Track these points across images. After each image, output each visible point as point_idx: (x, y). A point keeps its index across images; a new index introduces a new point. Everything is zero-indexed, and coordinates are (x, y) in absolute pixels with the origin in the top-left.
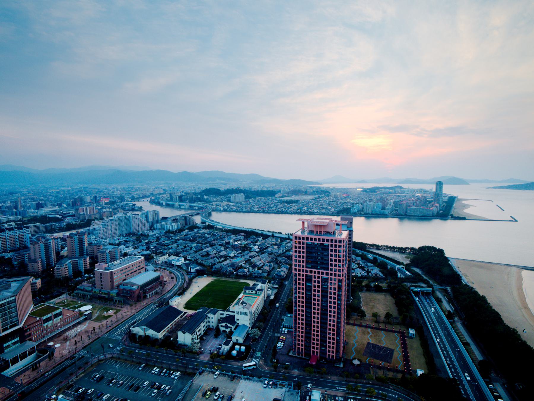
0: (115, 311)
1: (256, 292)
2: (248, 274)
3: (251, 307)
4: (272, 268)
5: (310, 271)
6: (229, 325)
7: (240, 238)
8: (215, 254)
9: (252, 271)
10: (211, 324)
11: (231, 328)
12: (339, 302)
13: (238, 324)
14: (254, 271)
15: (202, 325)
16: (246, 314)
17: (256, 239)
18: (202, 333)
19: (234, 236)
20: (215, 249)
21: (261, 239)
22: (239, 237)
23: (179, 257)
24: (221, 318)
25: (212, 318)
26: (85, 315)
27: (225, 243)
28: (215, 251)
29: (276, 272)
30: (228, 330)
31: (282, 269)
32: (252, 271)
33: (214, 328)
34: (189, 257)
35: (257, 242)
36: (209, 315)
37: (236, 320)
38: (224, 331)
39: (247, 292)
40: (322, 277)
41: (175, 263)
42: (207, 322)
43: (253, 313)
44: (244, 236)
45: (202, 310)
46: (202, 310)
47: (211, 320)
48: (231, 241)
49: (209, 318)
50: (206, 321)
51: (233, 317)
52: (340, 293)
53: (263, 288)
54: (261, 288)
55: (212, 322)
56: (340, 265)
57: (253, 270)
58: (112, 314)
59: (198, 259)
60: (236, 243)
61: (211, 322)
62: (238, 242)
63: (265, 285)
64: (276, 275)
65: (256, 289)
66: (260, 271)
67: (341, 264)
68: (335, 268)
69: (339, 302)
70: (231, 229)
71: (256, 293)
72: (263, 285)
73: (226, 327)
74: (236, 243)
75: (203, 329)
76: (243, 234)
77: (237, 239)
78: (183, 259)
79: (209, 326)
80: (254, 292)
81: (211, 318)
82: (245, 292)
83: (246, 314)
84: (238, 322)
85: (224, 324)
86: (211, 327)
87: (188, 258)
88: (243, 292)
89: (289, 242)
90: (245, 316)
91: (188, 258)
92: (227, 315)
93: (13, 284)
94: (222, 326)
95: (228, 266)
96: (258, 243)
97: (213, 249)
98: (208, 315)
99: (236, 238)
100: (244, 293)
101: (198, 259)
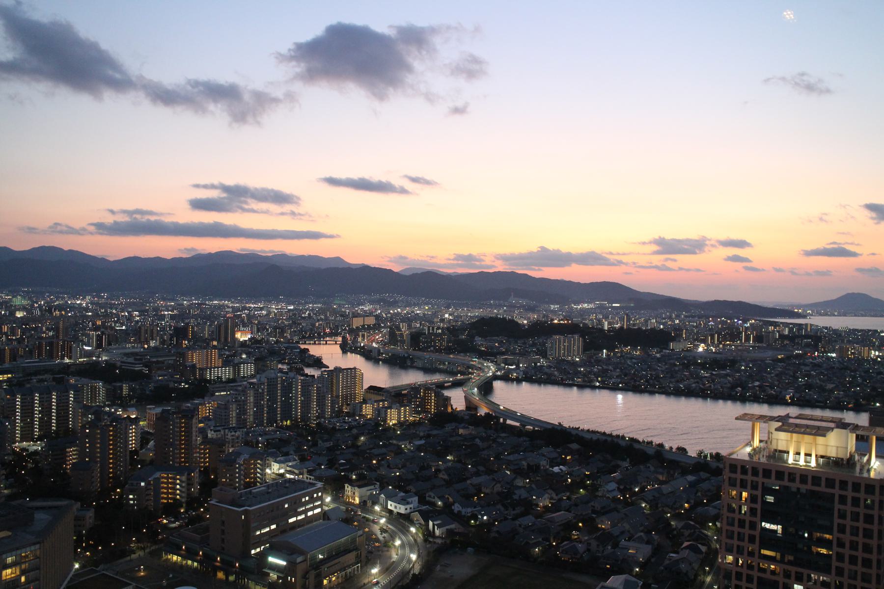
20: (500, 482)
23: (406, 492)
27: (526, 467)
34: (430, 496)
41: (396, 507)
48: (543, 463)
60: (556, 469)
62: (561, 467)
74: (556, 469)
78: (416, 499)
87: (427, 498)
89: (708, 479)
97: (494, 479)
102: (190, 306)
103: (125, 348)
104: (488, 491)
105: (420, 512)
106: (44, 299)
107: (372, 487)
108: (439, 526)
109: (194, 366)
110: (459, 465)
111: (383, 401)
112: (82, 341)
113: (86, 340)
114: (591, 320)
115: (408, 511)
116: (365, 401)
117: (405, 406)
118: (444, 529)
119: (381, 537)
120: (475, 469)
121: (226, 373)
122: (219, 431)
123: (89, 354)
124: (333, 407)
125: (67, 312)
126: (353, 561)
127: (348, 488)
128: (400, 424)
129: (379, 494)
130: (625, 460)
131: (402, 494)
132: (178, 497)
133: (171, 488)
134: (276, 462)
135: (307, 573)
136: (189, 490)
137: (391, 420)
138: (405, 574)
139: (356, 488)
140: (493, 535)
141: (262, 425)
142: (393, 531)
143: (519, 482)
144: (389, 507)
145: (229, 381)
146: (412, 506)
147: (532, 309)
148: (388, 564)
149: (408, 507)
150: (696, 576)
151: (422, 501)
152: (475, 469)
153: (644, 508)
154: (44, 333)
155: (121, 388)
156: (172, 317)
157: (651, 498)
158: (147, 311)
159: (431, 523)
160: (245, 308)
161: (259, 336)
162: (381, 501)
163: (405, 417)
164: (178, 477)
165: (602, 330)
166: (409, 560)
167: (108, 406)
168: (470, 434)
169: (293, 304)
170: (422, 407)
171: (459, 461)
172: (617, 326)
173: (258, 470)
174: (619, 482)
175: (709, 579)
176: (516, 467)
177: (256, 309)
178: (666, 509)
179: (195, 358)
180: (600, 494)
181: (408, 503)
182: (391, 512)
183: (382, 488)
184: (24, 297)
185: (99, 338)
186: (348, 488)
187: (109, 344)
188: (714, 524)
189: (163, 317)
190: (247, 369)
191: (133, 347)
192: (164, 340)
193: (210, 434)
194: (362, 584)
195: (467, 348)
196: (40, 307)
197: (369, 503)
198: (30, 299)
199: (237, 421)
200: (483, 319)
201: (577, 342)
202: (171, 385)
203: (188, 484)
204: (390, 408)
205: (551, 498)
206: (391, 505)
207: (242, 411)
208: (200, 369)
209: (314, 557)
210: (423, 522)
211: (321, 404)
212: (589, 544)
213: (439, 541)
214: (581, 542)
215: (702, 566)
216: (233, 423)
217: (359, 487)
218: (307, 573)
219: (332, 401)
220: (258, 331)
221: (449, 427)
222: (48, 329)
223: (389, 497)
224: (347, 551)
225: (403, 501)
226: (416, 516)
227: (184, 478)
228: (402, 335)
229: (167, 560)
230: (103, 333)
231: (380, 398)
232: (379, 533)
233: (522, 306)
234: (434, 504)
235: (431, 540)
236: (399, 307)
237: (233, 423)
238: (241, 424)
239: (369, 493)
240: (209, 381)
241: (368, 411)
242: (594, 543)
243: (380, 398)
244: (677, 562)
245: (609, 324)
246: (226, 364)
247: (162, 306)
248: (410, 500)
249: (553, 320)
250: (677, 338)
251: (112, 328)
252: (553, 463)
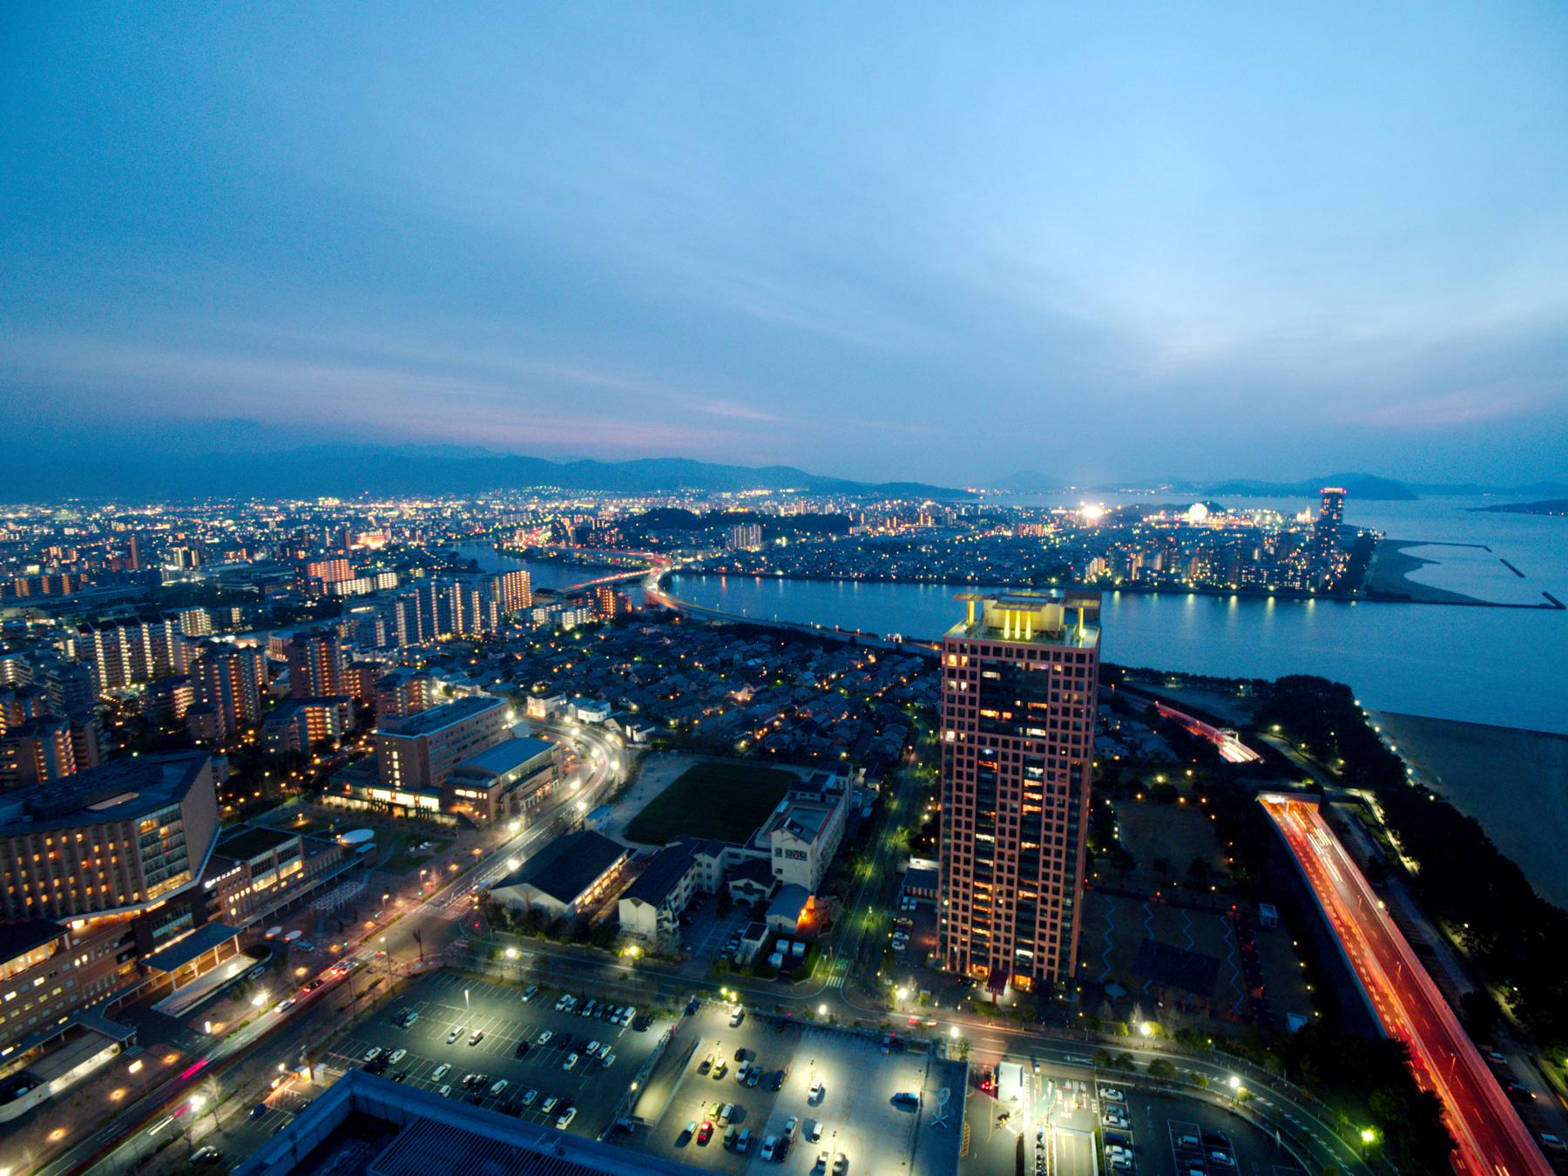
0: (436, 845)
1: (823, 799)
2: (792, 748)
3: (816, 838)
4: (859, 734)
5: (991, 739)
6: (756, 885)
7: (760, 650)
8: (696, 692)
9: (803, 741)
10: (705, 883)
11: (763, 892)
12: (1074, 826)
13: (781, 882)
14: (809, 740)
15: (683, 883)
16: (801, 856)
17: (807, 652)
18: (684, 906)
19: (742, 642)
20: (694, 680)
21: (820, 651)
22: (757, 646)
23: (596, 699)
24: (731, 866)
25: (709, 866)
26: (360, 854)
28: (694, 683)
29: (872, 745)
30: (753, 899)
31: (886, 735)
32: (803, 741)
33: (714, 892)
35: (810, 660)
36: (700, 857)
37: (774, 873)
38: (743, 902)
39: (798, 796)
40: (1024, 756)
42: (693, 878)
43: (819, 854)
44: (770, 642)
45: (678, 843)
46: (678, 843)
47: (704, 871)
48: (737, 657)
49: (700, 864)
50: (691, 872)
51: (768, 863)
52: (1076, 801)
53: (841, 788)
54: (835, 787)
55: (709, 877)
56: (1078, 725)
57: (806, 738)
58: (431, 853)
59: (649, 706)
60: (751, 663)
61: (705, 875)
63: (847, 779)
64: (872, 751)
65: (824, 789)
66: (825, 740)
67: (1082, 722)
68: (1065, 732)
69: (1074, 826)
70: (732, 623)
71: (823, 799)
72: (842, 779)
73: (748, 889)
74: (751, 663)
75: (684, 895)
76: (767, 637)
77: (751, 653)
78: (609, 705)
79: (700, 886)
80: (817, 797)
81: (704, 865)
82: (794, 796)
83: (801, 856)
84: (779, 877)
85: (741, 883)
86: (705, 889)
88: (787, 796)
90: (798, 862)
91: (621, 703)
92: (747, 857)
93: (168, 771)
94: (735, 888)
95: (736, 726)
96: (813, 664)
97: (688, 677)
98: (695, 856)
99: (748, 648)
100: (789, 800)
101: (649, 706)
102: (299, 510)
103: (224, 565)
104: (683, 690)
105: (616, 718)
106: (100, 511)
107: (559, 697)
108: (638, 731)
109: (320, 580)
110: (649, 666)
111: (556, 604)
112: (163, 560)
113: (168, 558)
114: (766, 507)
115: (601, 719)
116: (534, 606)
117: (581, 608)
118: (644, 733)
119: (575, 749)
120: (666, 669)
121: (362, 586)
122: (367, 652)
123: (176, 575)
124: (499, 614)
125: (135, 526)
126: (550, 777)
127: (530, 700)
128: (579, 628)
129: (568, 704)
130: (818, 648)
131: (593, 701)
132: (330, 732)
133: (319, 723)
134: (441, 680)
135: (501, 796)
136: (342, 722)
137: (567, 624)
138: (609, 784)
139: (541, 700)
140: (695, 734)
141: (418, 642)
142: (589, 742)
143: (714, 677)
144: (580, 717)
145: (367, 595)
146: (605, 713)
147: (702, 498)
148: (589, 777)
149: (602, 714)
150: (901, 755)
151: (616, 706)
152: (666, 669)
153: (843, 695)
154: (109, 553)
155: (230, 614)
156: (279, 524)
157: (849, 684)
158: (243, 518)
159: (628, 729)
160: (370, 510)
161: (395, 541)
162: (570, 711)
163: (582, 619)
164: (327, 709)
165: (778, 517)
166: (610, 771)
167: (216, 635)
168: (656, 632)
169: (430, 501)
170: (599, 606)
171: (649, 662)
172: (794, 513)
173: (424, 692)
174: (816, 670)
175: (913, 757)
176: (710, 663)
177: (385, 510)
178: (864, 694)
179: (319, 570)
180: (797, 683)
181: (601, 710)
182: (582, 722)
183: (570, 698)
184: (70, 510)
185: (187, 556)
186: (530, 700)
187: (202, 561)
188: (912, 705)
189: (266, 525)
190: (388, 580)
191: (235, 563)
192: (274, 553)
193: (356, 658)
194: (563, 800)
195: (638, 544)
196: (96, 521)
197: (557, 714)
198: (81, 511)
199: (386, 639)
200: (654, 510)
201: (756, 531)
202: (294, 604)
203: (341, 716)
204: (565, 610)
205: (750, 692)
206: (583, 714)
207: (391, 627)
208: (328, 583)
209: (506, 779)
210: (619, 729)
211: (485, 609)
212: (794, 735)
213: (639, 746)
214: (785, 733)
215: (905, 745)
216: (382, 642)
217: (544, 698)
218: (501, 796)
219: (497, 608)
220: (393, 534)
221: (632, 627)
222: (113, 548)
223: (580, 706)
224: (542, 768)
225: (596, 708)
226: (611, 723)
227: (335, 710)
228: (566, 532)
229: (329, 804)
230: (191, 549)
231: (552, 601)
232: (573, 744)
233: (692, 495)
234: (628, 709)
235: (631, 746)
236: (557, 501)
237: (382, 642)
238: (392, 642)
239: (555, 704)
240: (342, 597)
241: (540, 616)
242: (799, 733)
243: (552, 601)
244: (882, 744)
245: (786, 510)
246: (360, 575)
247: (261, 512)
248: (602, 707)
249: (727, 509)
250: (856, 523)
251: (202, 542)
252: (746, 656)
